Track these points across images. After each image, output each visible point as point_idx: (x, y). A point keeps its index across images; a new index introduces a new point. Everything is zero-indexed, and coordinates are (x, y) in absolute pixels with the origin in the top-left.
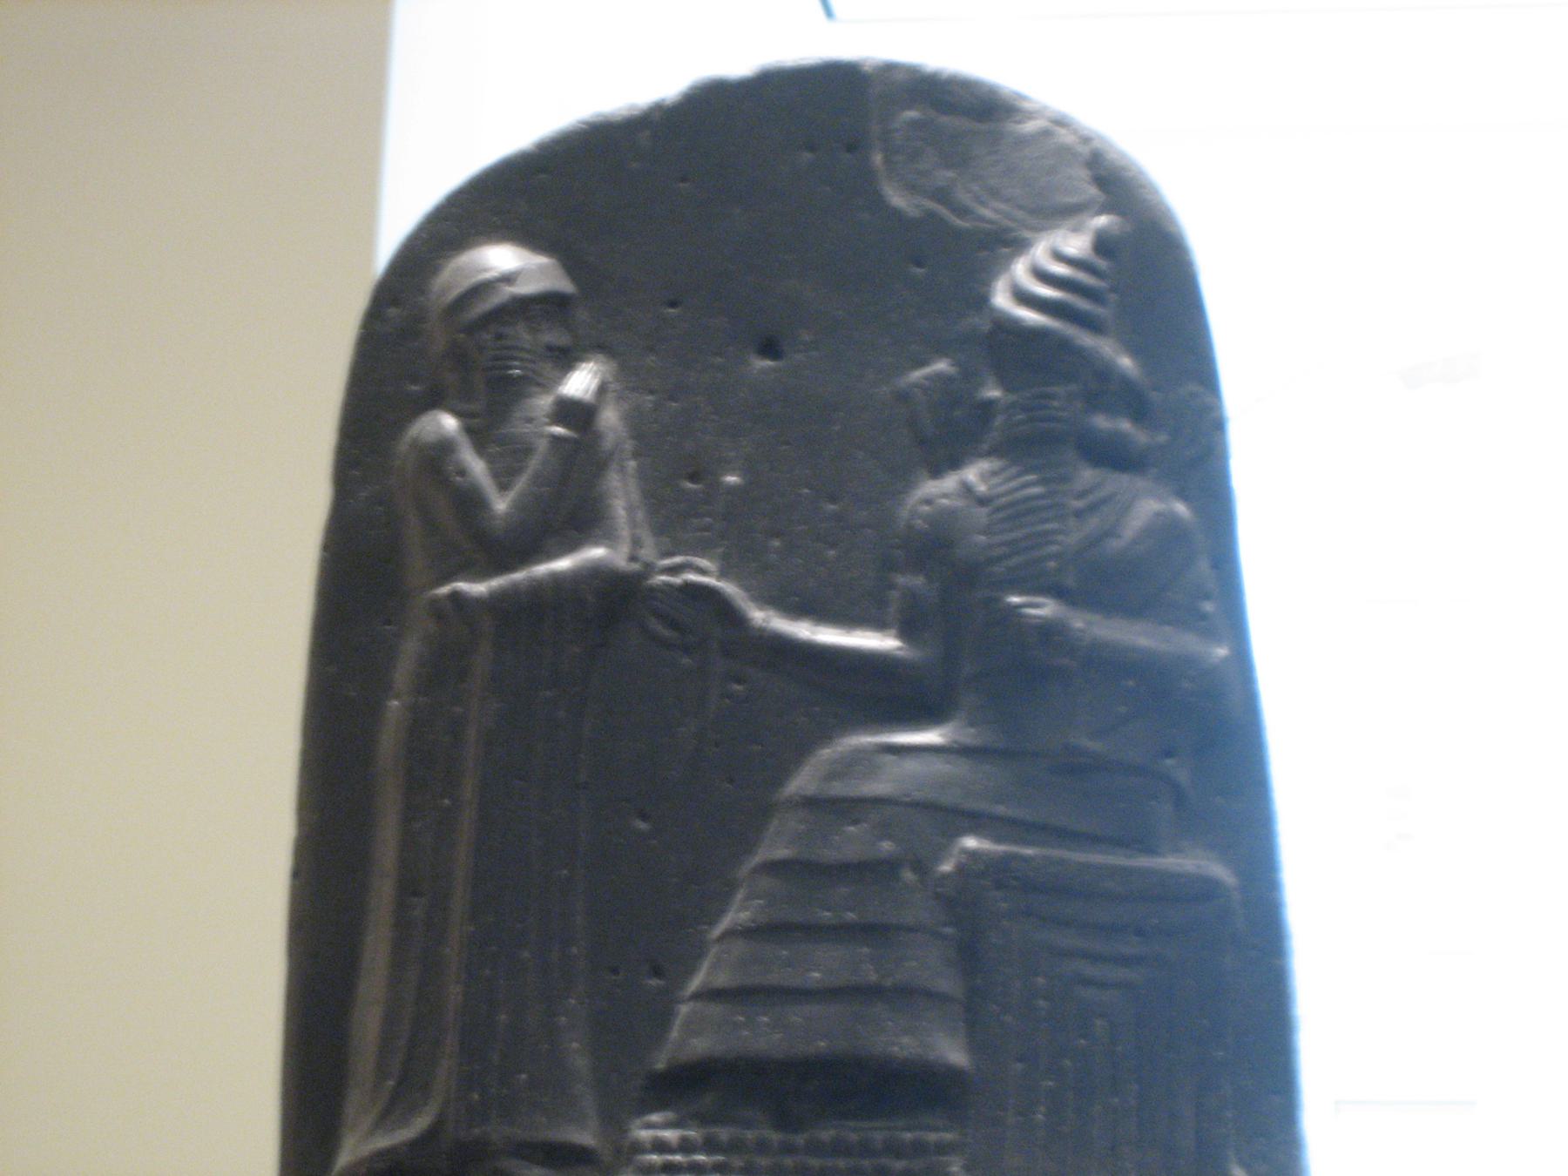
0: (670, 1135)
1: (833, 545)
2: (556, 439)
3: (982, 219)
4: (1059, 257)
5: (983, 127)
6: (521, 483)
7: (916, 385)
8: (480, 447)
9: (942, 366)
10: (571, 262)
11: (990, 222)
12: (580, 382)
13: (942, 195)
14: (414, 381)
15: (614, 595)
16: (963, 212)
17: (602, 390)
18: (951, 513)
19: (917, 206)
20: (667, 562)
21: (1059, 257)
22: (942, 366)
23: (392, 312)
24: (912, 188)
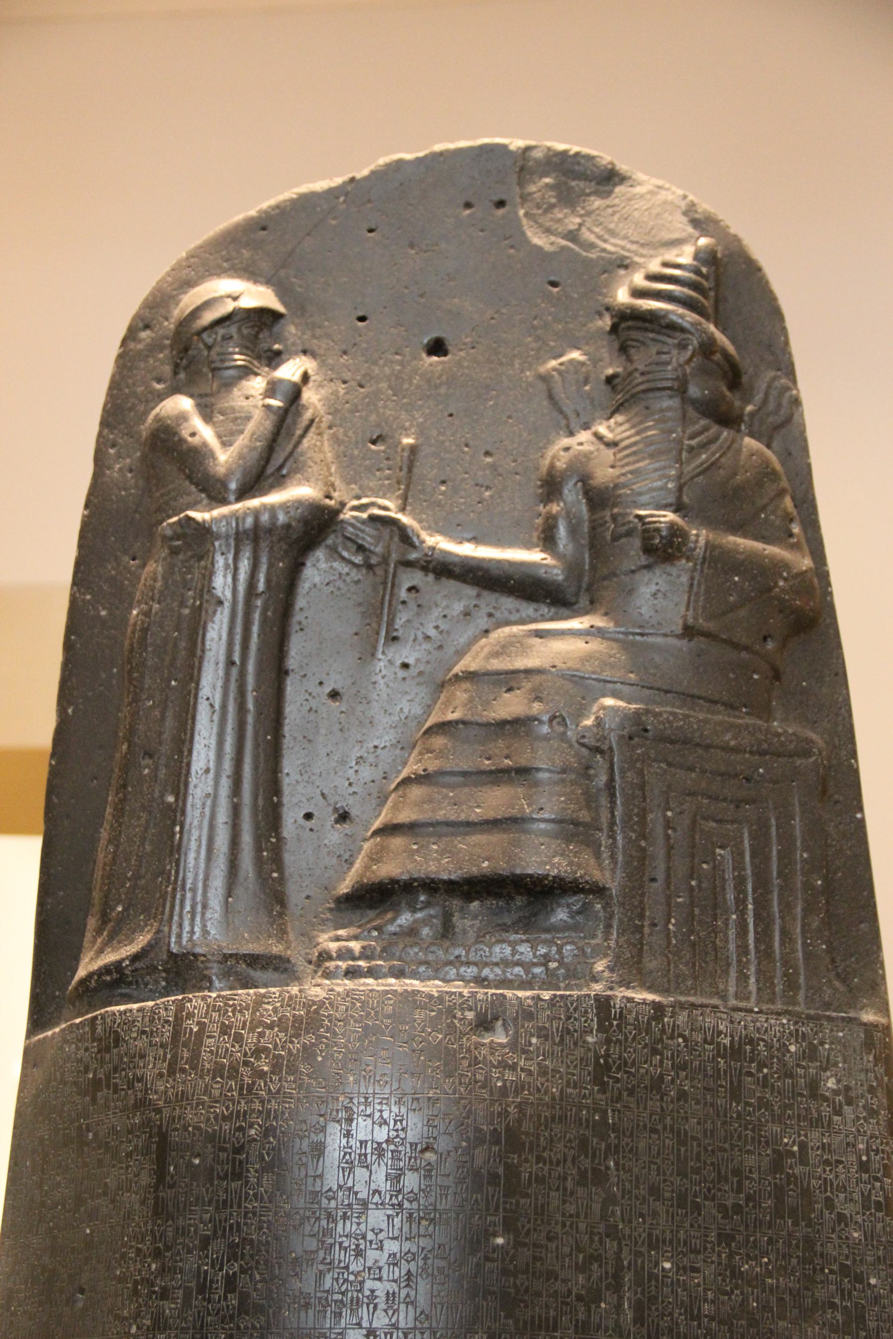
0: (356, 946)
1: (488, 488)
2: (268, 407)
3: (604, 250)
4: (666, 265)
5: (606, 188)
6: (241, 441)
7: (554, 369)
9: (575, 355)
10: (282, 292)
11: (613, 253)
12: (290, 370)
13: (573, 236)
14: (159, 381)
15: (316, 526)
17: (306, 377)
18: (587, 456)
19: (552, 244)
20: (355, 503)
22: (575, 355)
23: (144, 335)
24: (548, 231)
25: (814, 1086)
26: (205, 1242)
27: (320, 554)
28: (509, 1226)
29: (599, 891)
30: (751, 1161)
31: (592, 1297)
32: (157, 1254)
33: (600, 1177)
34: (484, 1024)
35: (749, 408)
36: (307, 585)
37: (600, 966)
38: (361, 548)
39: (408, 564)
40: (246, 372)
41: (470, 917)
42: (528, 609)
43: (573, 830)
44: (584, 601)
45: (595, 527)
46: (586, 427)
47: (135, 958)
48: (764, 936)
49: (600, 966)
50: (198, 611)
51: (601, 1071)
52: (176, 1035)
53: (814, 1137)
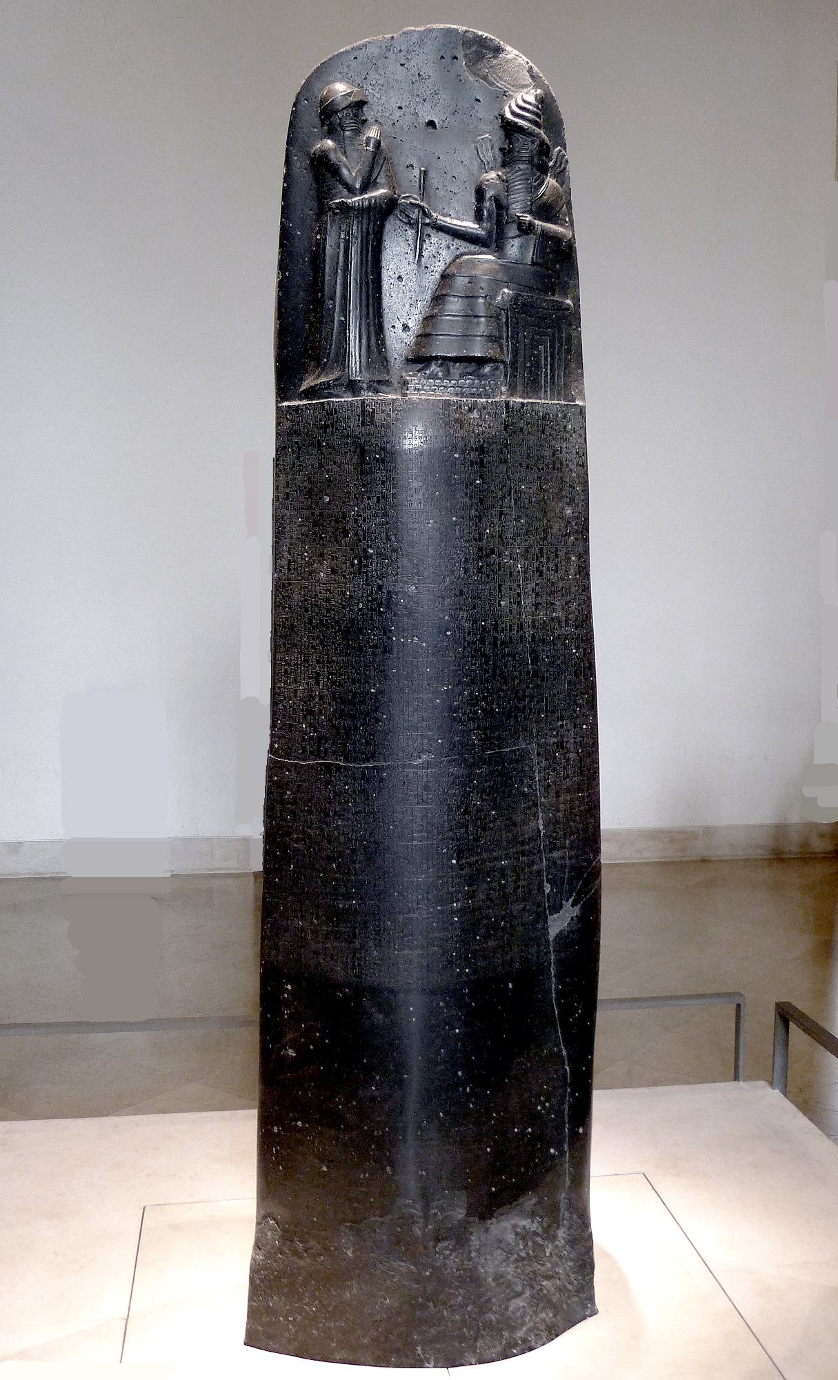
4: (525, 101)
8: (345, 153)
12: (373, 132)
16: (492, 84)
21: (525, 101)
25: (565, 427)
26: (383, 483)
27: (391, 217)
28: (481, 477)
29: (503, 362)
30: (547, 454)
31: (503, 497)
32: (364, 486)
33: (506, 461)
34: (470, 410)
35: (551, 164)
36: (386, 230)
37: (504, 389)
38: (407, 216)
39: (427, 225)
40: (358, 132)
41: (457, 369)
42: (472, 248)
43: (493, 339)
44: (494, 246)
45: (499, 215)
46: (492, 169)
47: (335, 380)
48: (552, 376)
49: (504, 389)
50: (347, 242)
51: (506, 426)
52: (363, 411)
53: (564, 445)
